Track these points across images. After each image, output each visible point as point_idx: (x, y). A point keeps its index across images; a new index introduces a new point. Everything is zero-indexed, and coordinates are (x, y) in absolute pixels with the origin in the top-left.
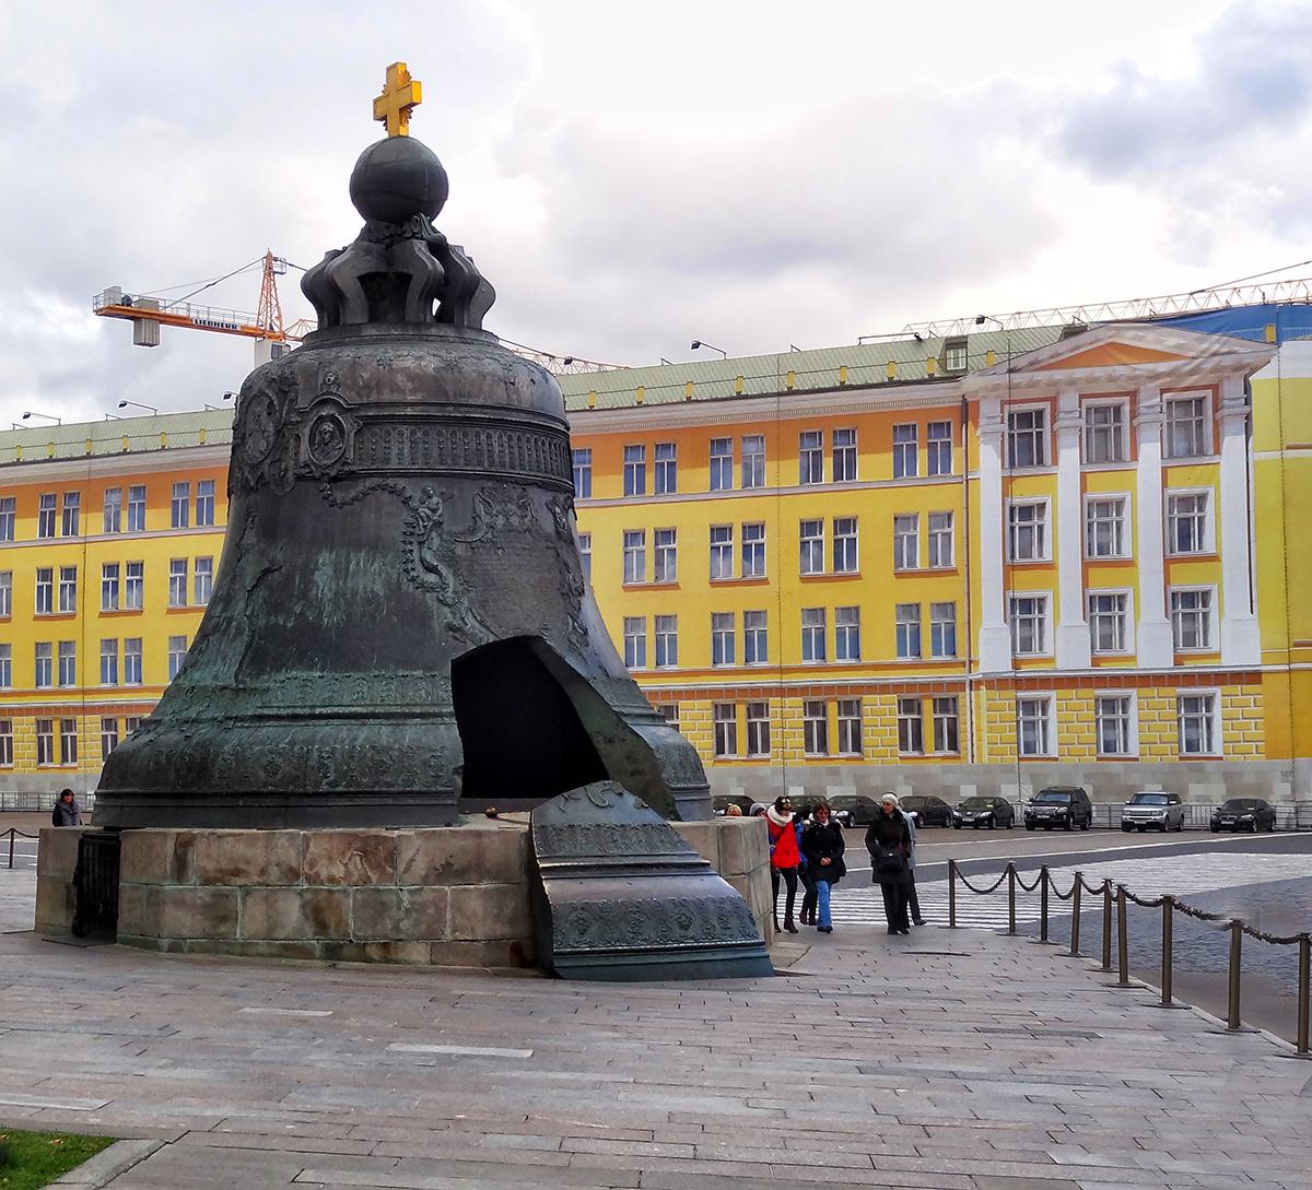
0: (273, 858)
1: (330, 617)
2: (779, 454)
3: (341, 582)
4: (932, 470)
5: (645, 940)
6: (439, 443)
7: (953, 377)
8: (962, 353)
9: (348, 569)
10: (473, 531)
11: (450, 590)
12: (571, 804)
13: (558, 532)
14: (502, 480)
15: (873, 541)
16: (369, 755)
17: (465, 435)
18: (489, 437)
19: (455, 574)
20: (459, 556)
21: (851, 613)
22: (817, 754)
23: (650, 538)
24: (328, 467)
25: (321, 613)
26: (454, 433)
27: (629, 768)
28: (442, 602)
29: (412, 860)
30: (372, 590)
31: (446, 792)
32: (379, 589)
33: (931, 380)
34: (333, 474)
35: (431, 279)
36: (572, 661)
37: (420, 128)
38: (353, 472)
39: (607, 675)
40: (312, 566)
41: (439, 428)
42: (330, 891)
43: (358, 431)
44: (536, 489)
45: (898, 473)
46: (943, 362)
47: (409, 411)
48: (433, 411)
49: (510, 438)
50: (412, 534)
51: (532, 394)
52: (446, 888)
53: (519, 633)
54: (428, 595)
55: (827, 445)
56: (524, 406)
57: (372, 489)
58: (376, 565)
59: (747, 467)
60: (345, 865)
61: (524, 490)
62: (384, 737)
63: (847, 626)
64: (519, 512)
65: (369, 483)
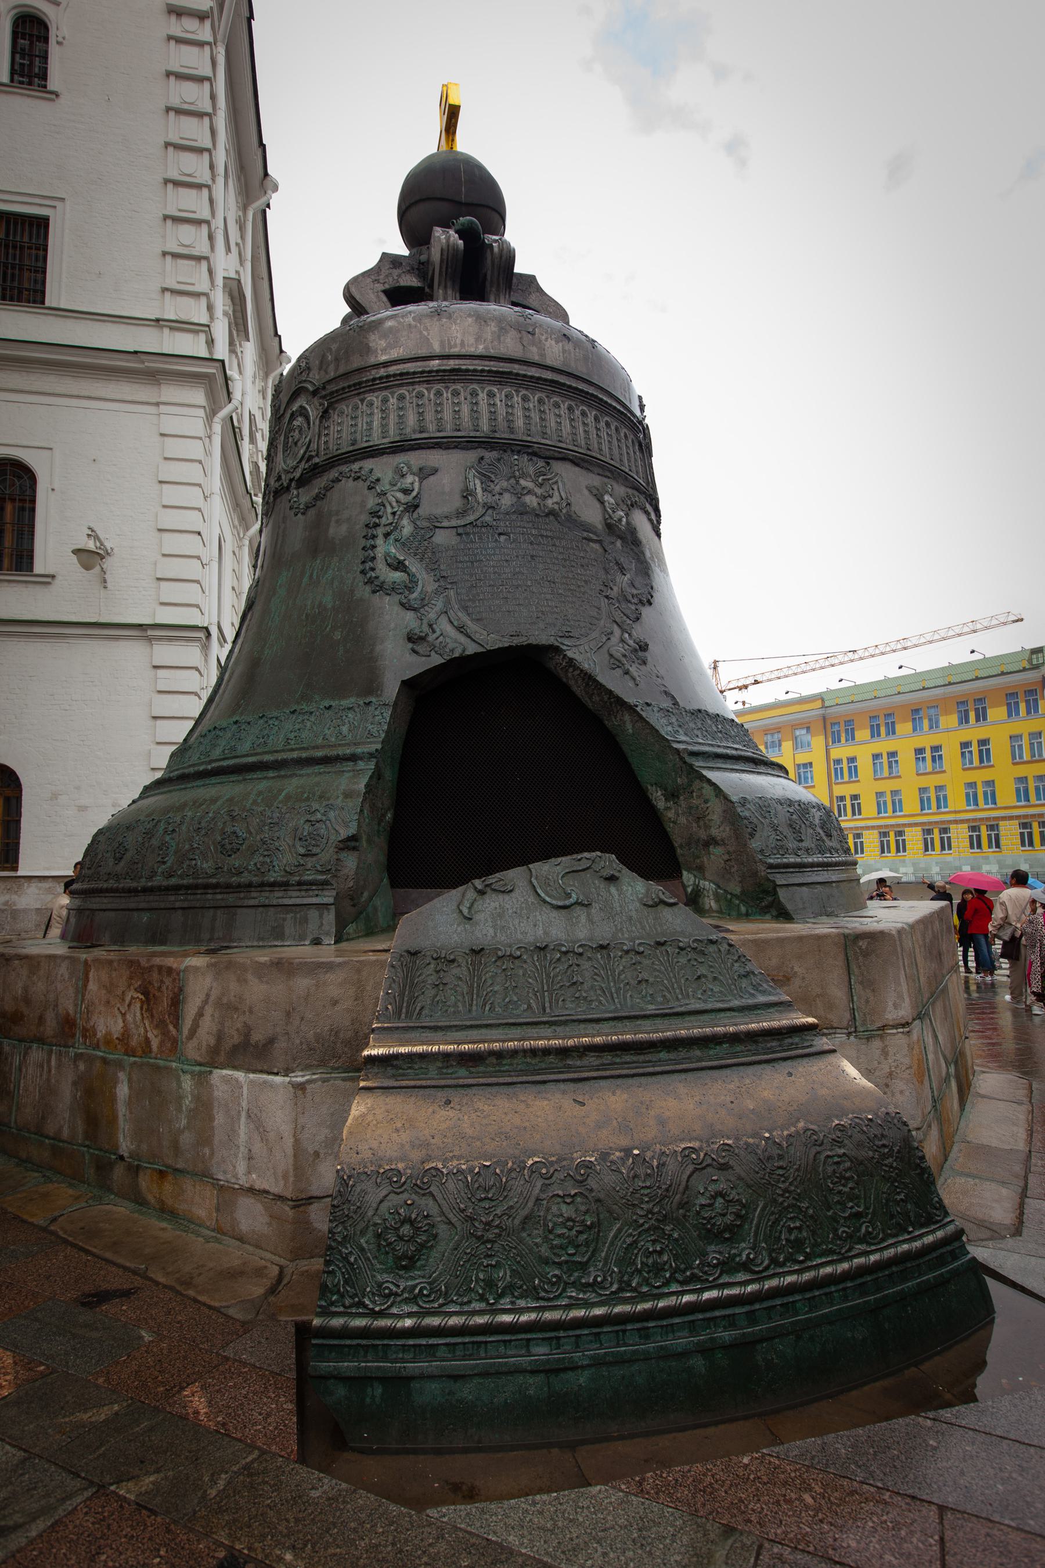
0: (52, 997)
2: (947, 713)
4: (1028, 712)
5: (593, 1286)
6: (418, 405)
7: (1037, 667)
8: (1040, 655)
11: (419, 589)
12: (491, 903)
15: (1000, 750)
16: (220, 825)
17: (456, 394)
21: (990, 783)
22: (976, 850)
23: (885, 756)
24: (295, 468)
26: (439, 394)
28: (406, 606)
29: (200, 1014)
30: (321, 603)
32: (328, 600)
33: (1024, 670)
34: (297, 474)
35: (445, 254)
39: (676, 704)
41: (419, 388)
42: (105, 1061)
44: (568, 466)
45: (1010, 715)
46: (1030, 661)
47: (382, 372)
48: (410, 367)
49: (525, 399)
50: (376, 525)
51: (564, 351)
52: (240, 1075)
53: (516, 641)
55: (971, 706)
56: (549, 362)
57: (333, 481)
59: (930, 720)
60: (124, 1015)
61: (548, 464)
62: (252, 796)
63: (989, 790)
64: (538, 491)
65: (334, 474)
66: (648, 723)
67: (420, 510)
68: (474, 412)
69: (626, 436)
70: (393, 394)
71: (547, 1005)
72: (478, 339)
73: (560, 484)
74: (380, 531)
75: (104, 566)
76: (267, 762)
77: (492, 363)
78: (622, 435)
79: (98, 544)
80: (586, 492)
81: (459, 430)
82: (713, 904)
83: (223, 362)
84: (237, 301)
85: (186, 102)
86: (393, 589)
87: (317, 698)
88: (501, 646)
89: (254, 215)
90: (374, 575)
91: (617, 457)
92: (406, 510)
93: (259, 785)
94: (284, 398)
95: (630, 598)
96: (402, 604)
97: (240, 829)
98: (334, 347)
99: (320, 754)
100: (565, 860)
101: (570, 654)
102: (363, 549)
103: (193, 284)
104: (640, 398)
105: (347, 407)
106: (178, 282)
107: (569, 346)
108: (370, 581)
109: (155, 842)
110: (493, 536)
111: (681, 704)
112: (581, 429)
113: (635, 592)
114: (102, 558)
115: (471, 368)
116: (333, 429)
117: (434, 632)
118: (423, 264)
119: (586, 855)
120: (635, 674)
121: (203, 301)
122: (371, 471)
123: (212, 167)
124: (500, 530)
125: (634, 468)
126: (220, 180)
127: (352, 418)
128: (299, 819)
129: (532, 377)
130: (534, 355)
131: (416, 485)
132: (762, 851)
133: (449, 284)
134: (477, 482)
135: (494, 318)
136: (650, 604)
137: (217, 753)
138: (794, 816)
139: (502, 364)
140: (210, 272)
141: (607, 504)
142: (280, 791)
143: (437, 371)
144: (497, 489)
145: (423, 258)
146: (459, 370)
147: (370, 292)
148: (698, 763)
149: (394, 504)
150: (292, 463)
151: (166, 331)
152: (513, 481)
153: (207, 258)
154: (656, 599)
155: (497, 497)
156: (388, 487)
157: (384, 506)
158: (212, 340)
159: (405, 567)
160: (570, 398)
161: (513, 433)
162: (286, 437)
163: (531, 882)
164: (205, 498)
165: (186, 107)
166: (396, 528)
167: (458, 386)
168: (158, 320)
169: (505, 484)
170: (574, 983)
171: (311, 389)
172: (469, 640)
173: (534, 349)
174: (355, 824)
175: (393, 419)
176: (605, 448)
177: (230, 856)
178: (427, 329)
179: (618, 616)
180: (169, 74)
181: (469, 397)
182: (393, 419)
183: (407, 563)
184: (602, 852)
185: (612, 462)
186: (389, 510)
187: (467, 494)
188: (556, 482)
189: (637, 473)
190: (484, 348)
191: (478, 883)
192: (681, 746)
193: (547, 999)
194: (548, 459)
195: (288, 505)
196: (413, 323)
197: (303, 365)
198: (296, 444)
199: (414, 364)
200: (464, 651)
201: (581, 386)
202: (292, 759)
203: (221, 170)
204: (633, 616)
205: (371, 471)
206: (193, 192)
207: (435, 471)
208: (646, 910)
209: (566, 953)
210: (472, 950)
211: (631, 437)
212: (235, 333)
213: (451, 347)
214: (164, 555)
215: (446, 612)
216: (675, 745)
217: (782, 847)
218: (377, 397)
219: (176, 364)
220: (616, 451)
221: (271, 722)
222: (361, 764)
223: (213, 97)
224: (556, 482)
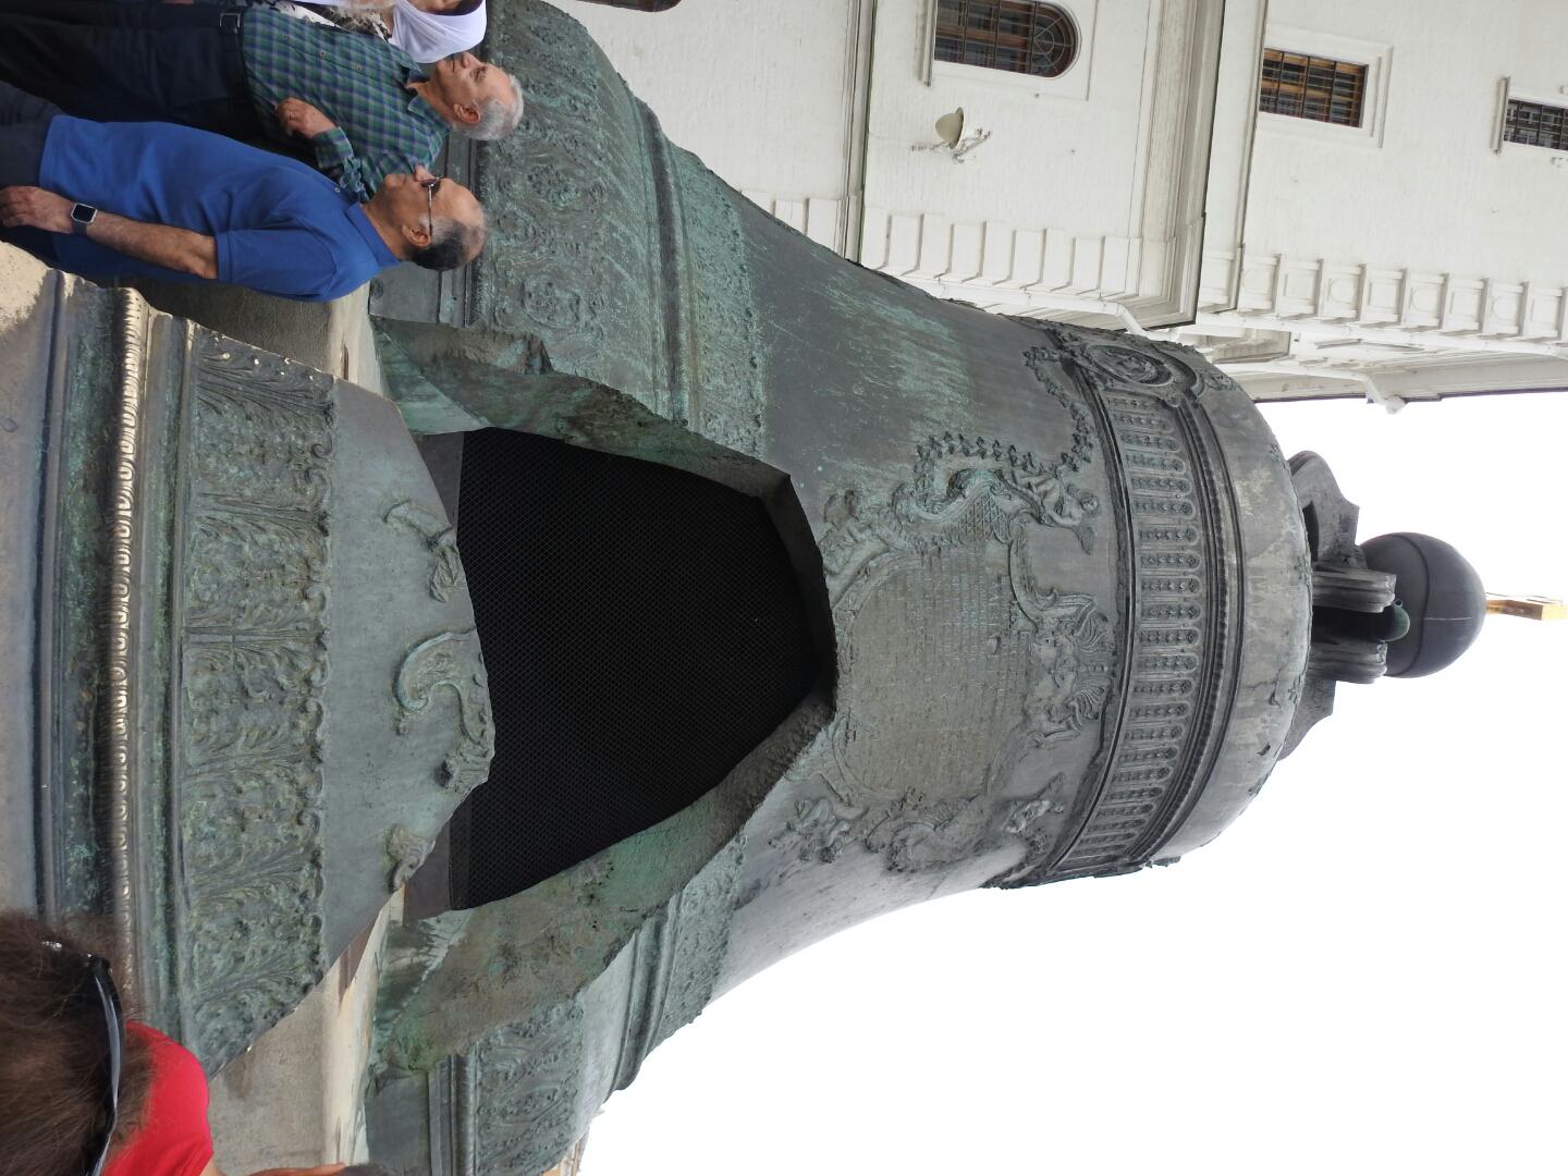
1: (841, 297)
3: (905, 333)
6: (1176, 533)
9: (928, 348)
10: (1029, 586)
11: (924, 515)
12: (411, 557)
13: (1003, 805)
14: (1114, 665)
17: (1192, 586)
18: (1190, 637)
19: (950, 532)
20: (984, 546)
25: (847, 292)
26: (1192, 562)
27: (520, 943)
28: (897, 493)
31: (474, 301)
34: (1080, 361)
36: (780, 795)
37: (1493, 629)
38: (1091, 386)
39: (739, 904)
40: (919, 311)
41: (1199, 532)
43: (1164, 405)
44: (1092, 747)
47: (1219, 485)
48: (1227, 525)
49: (1185, 686)
50: (1013, 461)
51: (1247, 746)
53: (843, 654)
54: (910, 467)
56: (1233, 723)
57: (1072, 406)
58: (948, 391)
62: (622, 228)
64: (1057, 701)
65: (1084, 410)
66: (710, 858)
67: (1033, 526)
68: (1167, 612)
69: (1129, 836)
70: (1191, 497)
71: (206, 638)
72: (1265, 622)
73: (1068, 733)
74: (1004, 464)
75: (940, 149)
76: (674, 259)
77: (1233, 640)
78: (1131, 831)
79: (968, 144)
80: (1054, 773)
81: (1143, 588)
82: (405, 961)
83: (1193, 322)
84: (1261, 351)
85: (1493, 303)
86: (922, 478)
87: (768, 349)
88: (837, 630)
89: (1360, 382)
90: (945, 450)
91: (1103, 821)
92: (1031, 501)
93: (644, 245)
94: (1178, 355)
95: (902, 834)
96: (901, 487)
97: (571, 197)
98: (1249, 423)
99: (683, 336)
100: (484, 693)
101: (821, 736)
102: (981, 440)
103: (1285, 295)
104: (1177, 859)
105: (1172, 435)
106: (1287, 276)
107: (1253, 752)
108: (933, 443)
109: (559, 81)
110: (997, 629)
111: (739, 912)
112: (1143, 768)
113: (910, 842)
114: (952, 146)
115: (1227, 610)
116: (1144, 414)
117: (861, 531)
118: (1346, 560)
119: (491, 730)
120: (787, 840)
121: (1266, 305)
122: (1087, 460)
123: (1421, 329)
124: (1004, 641)
125: (1085, 847)
126: (1403, 339)
127: (1158, 439)
128: (581, 287)
129: (1214, 697)
130: (1244, 701)
131: (1067, 522)
132: (487, 1046)
133: (1326, 591)
134: (1073, 610)
135: (1291, 645)
136: (890, 869)
137: (690, 200)
138: (545, 1103)
139: (1232, 653)
140: (1299, 317)
141: (1036, 804)
142: (629, 268)
143: (1222, 562)
144: (1062, 639)
145: (1353, 560)
146: (1224, 592)
147: (1311, 486)
148: (644, 936)
149: (1042, 488)
150: (1095, 355)
151: (1229, 256)
152: (1073, 662)
153: (1315, 312)
154: (895, 879)
155: (1051, 638)
156: (1066, 481)
157: (1040, 474)
158: (1218, 312)
159: (955, 497)
160: (1185, 751)
161: (1139, 666)
162: (1128, 352)
163: (444, 632)
164: (1025, 287)
165: (1489, 302)
166: (1009, 487)
167: (1202, 590)
168: (1242, 246)
169: (1069, 651)
170: (245, 693)
171: (1193, 388)
172: (846, 581)
173: (1251, 703)
174: (570, 371)
175: (1158, 495)
176: (1117, 804)
177: (530, 178)
178: (1277, 550)
179: (875, 815)
180: (1524, 285)
181: (1188, 604)
182: (1158, 495)
183: (960, 500)
184: (493, 762)
185: (1094, 814)
186: (1034, 480)
187: (1055, 595)
188: (1069, 727)
189: (1077, 853)
190: (1253, 631)
191: (450, 538)
192: (671, 910)
193: (219, 639)
194: (1102, 718)
195: (1038, 344)
196: (1284, 532)
197: (1223, 382)
198: (1120, 363)
199: (1231, 530)
200: (833, 574)
201: (1200, 769)
202: (677, 296)
203: (1416, 340)
204: (874, 840)
205: (1087, 460)
206: (1392, 303)
207: (1087, 549)
208: (382, 832)
209: (308, 681)
210: (323, 516)
211: (1128, 843)
212: (1223, 346)
213: (1255, 582)
214: (952, 227)
215: (888, 551)
216: (673, 902)
217: (494, 1081)
218: (1186, 475)
219: (1190, 263)
220: (1110, 820)
221: (735, 279)
222: (665, 396)
223: (1500, 337)
224: (1069, 727)
